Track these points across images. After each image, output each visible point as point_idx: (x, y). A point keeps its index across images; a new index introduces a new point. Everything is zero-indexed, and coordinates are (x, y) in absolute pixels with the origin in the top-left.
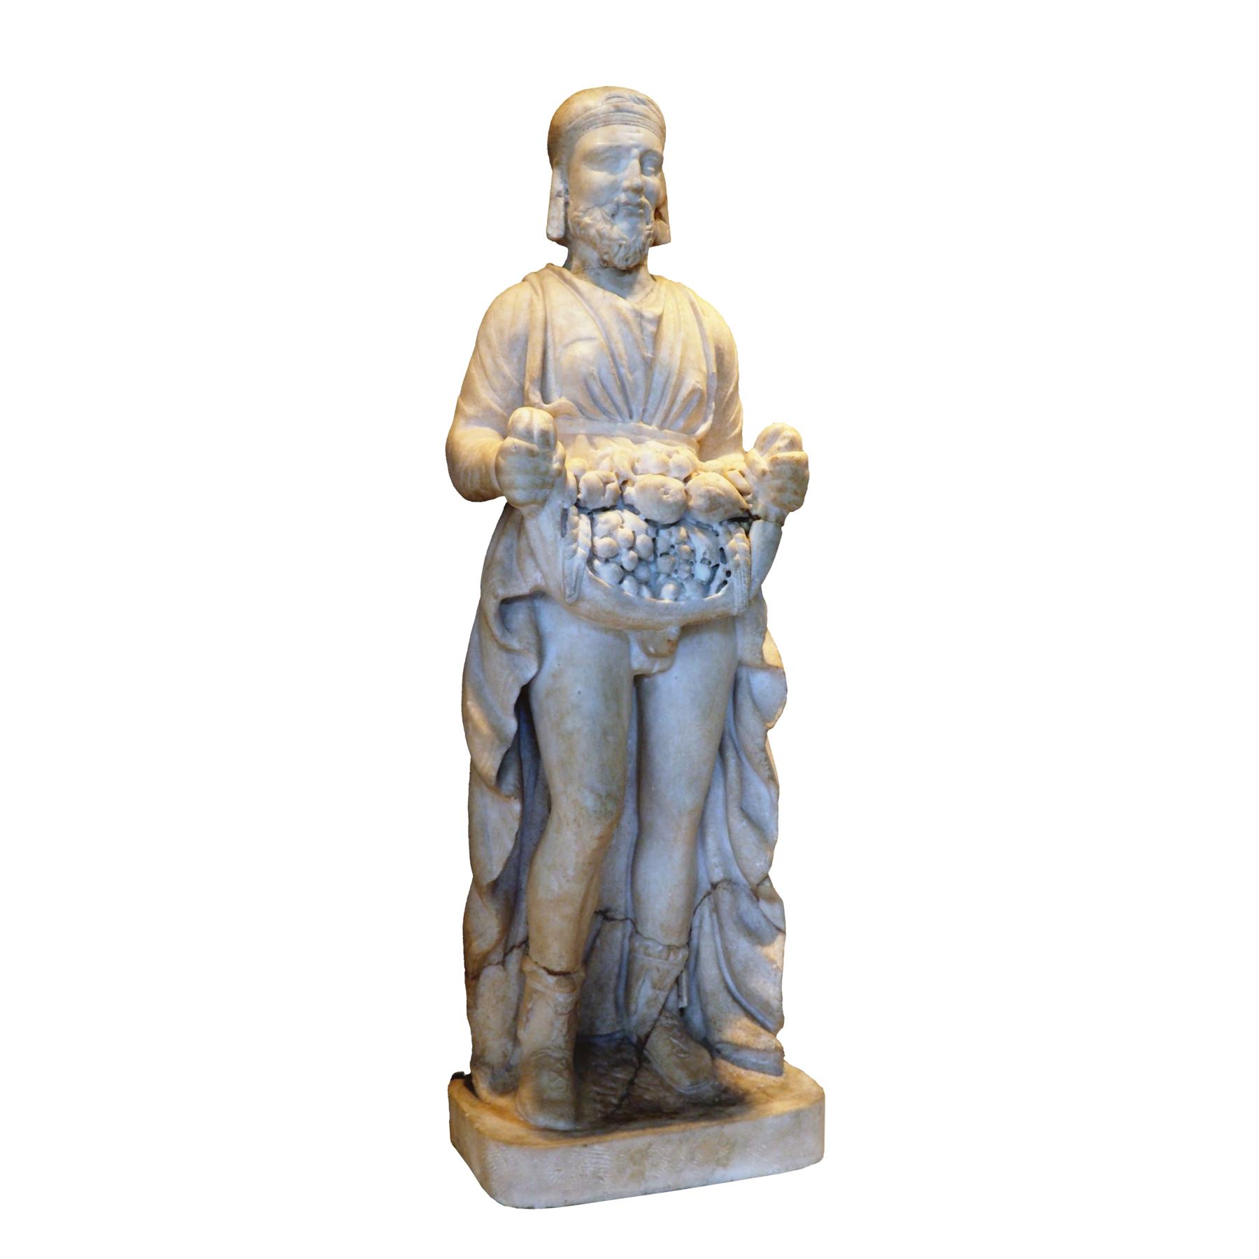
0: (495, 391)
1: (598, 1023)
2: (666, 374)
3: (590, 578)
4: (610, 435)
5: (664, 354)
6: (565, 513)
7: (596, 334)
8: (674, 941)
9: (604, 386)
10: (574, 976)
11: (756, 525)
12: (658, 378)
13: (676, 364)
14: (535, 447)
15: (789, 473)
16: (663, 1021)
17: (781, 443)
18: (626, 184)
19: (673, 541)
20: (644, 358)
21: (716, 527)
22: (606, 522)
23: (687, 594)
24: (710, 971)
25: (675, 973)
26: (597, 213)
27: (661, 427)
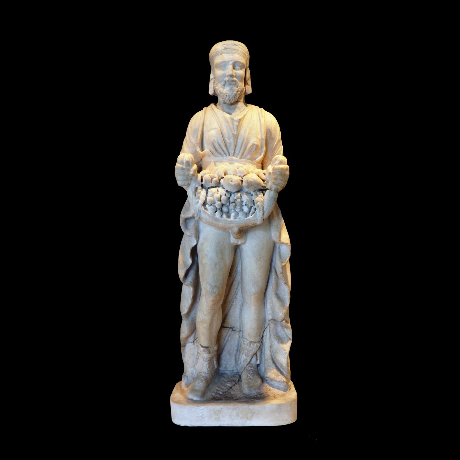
0: (189, 148)
1: (228, 366)
2: (242, 139)
3: (203, 211)
4: (221, 162)
5: (242, 133)
6: (196, 189)
7: (217, 127)
8: (252, 340)
9: (219, 145)
10: (211, 349)
11: (267, 193)
12: (240, 141)
13: (246, 135)
14: (184, 167)
15: (278, 173)
16: (248, 368)
17: (277, 162)
18: (227, 74)
19: (236, 198)
20: (233, 134)
21: (253, 193)
22: (211, 192)
23: (240, 217)
24: (267, 352)
25: (254, 351)
26: (220, 85)
27: (241, 158)
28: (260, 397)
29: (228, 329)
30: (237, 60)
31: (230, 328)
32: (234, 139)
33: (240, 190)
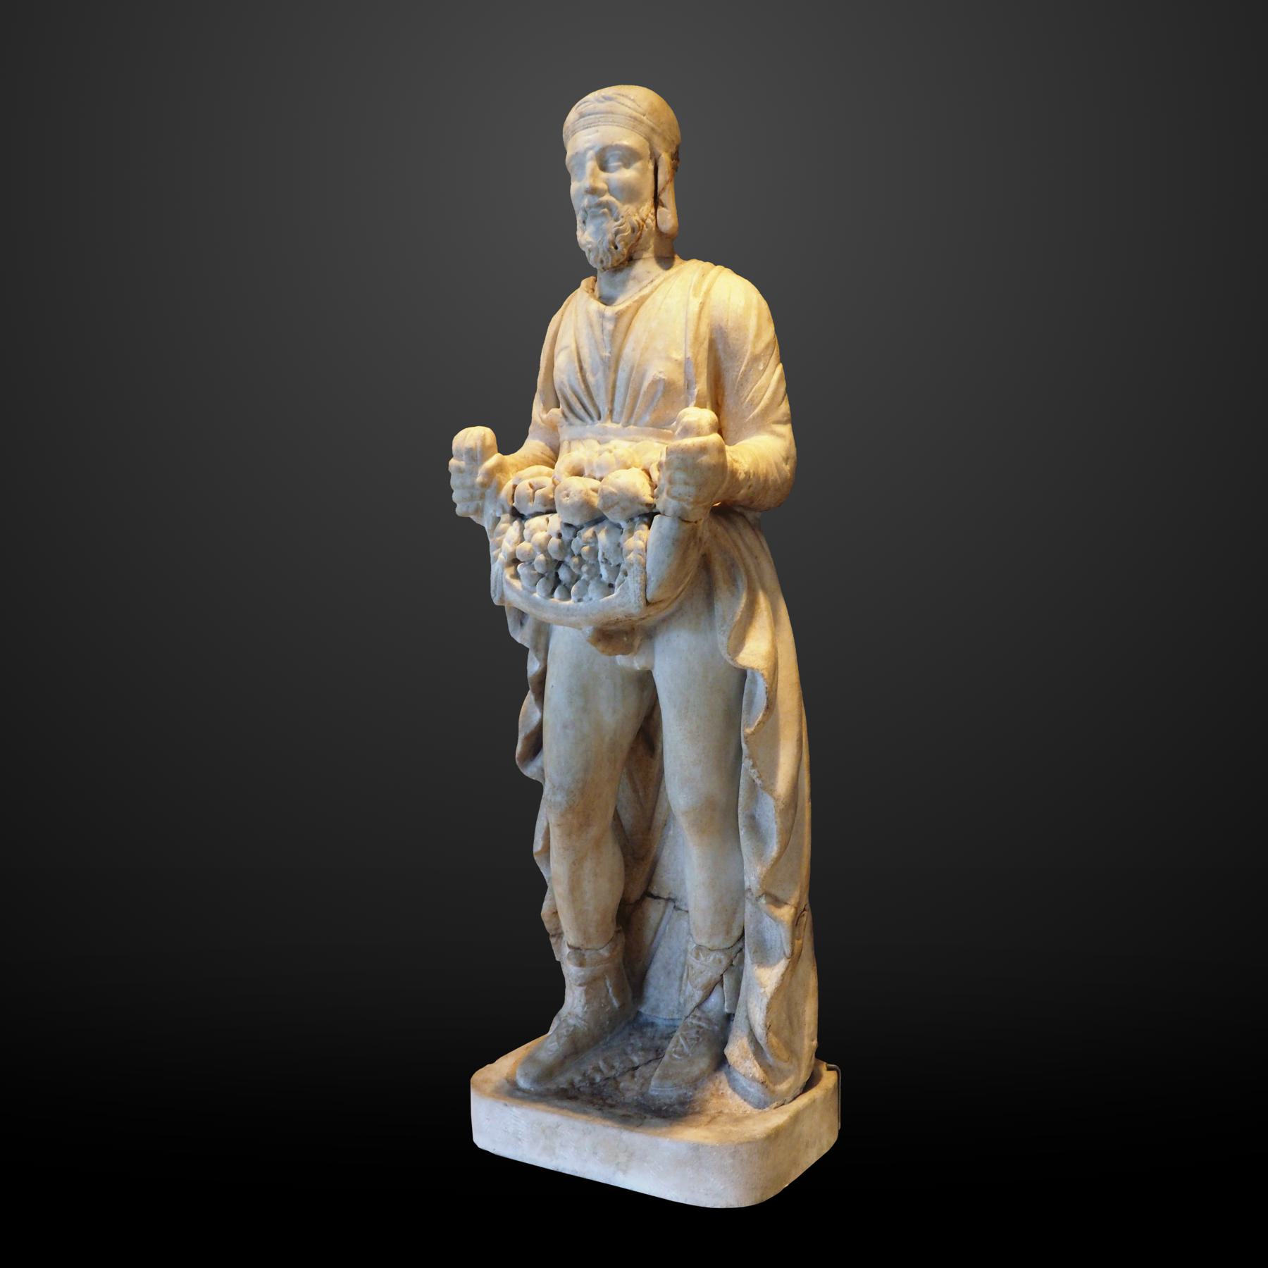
1: (662, 1005)
5: (627, 351)
10: (587, 954)
12: (622, 375)
20: (602, 359)
21: (623, 524)
28: (673, 1112)
29: (662, 902)
30: (608, 142)
31: (669, 900)
32: (606, 377)
33: (597, 519)
